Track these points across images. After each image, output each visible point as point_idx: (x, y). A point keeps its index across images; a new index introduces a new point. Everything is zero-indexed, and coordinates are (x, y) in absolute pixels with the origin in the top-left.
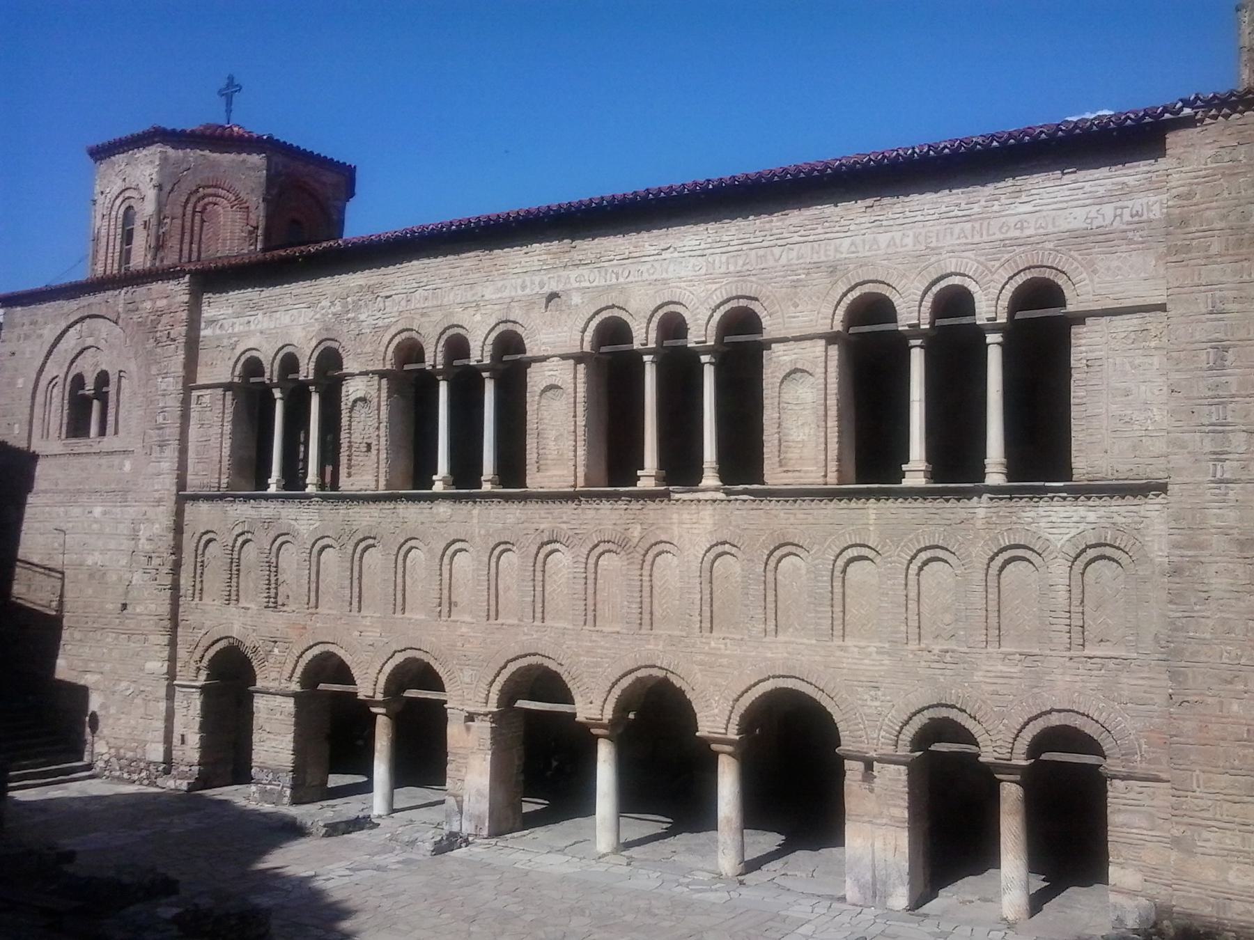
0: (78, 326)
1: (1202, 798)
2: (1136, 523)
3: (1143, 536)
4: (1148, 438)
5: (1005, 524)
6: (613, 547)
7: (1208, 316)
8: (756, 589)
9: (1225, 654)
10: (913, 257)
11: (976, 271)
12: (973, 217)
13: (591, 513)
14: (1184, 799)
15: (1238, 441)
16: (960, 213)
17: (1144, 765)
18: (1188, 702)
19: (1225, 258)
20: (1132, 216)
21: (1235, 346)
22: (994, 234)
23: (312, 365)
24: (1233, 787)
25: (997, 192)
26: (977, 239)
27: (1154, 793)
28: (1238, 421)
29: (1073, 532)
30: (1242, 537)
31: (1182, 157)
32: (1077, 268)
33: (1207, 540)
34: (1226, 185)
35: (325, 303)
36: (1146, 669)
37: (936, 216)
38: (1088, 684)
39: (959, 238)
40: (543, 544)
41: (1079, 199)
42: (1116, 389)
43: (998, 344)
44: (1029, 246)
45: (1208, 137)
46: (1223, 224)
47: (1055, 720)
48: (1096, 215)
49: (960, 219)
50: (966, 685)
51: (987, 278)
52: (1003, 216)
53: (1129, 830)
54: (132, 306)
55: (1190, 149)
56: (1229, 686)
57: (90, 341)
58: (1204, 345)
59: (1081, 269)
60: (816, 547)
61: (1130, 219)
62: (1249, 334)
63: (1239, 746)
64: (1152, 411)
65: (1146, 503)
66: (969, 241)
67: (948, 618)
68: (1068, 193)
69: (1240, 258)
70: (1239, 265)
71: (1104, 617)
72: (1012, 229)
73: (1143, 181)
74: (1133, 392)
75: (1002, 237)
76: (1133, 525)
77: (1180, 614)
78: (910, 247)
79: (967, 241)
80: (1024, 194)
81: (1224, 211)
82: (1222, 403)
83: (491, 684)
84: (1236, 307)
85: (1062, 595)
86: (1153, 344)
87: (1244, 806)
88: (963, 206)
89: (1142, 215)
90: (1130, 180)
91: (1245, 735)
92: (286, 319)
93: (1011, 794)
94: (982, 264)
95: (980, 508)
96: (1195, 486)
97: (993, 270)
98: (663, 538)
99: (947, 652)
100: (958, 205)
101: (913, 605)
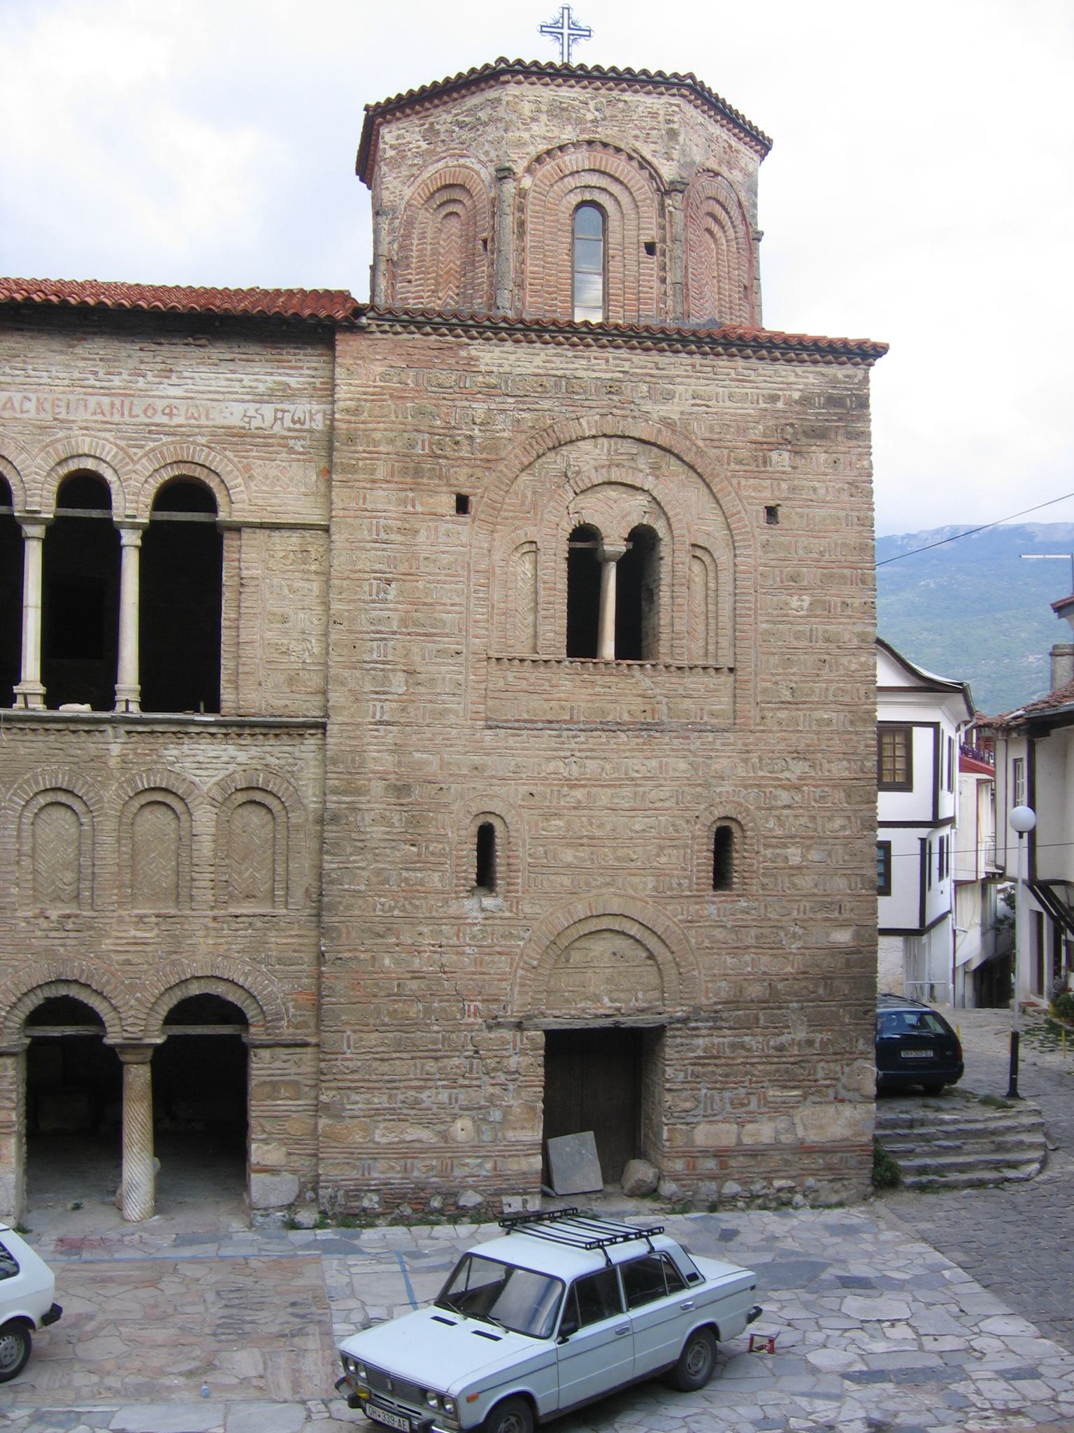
1: (351, 1060)
2: (290, 765)
3: (297, 779)
4: (304, 672)
5: (145, 763)
7: (372, 544)
9: (379, 906)
10: (34, 426)
11: (115, 456)
12: (113, 391)
14: (333, 1063)
15: (398, 684)
16: (98, 384)
17: (291, 1030)
18: (340, 959)
19: (390, 485)
20: (294, 422)
21: (397, 580)
22: (138, 416)
24: (383, 1044)
25: (142, 367)
26: (117, 418)
27: (301, 1059)
28: (397, 659)
29: (222, 774)
30: (399, 783)
31: (351, 368)
32: (232, 471)
33: (365, 785)
34: (393, 407)
36: (296, 926)
37: (66, 382)
38: (233, 946)
39: (95, 413)
41: (237, 393)
42: (274, 614)
43: (136, 546)
44: (178, 438)
45: (378, 353)
46: (390, 449)
47: (195, 989)
48: (254, 414)
49: (96, 390)
50: (92, 955)
51: (129, 468)
52: (150, 397)
53: (274, 1103)
55: (359, 362)
56: (379, 941)
58: (367, 576)
59: (236, 473)
61: (292, 426)
62: (411, 568)
63: (389, 1001)
64: (311, 642)
65: (302, 744)
66: (108, 419)
67: (69, 876)
68: (225, 383)
69: (405, 486)
70: (403, 495)
71: (251, 870)
72: (159, 413)
73: (307, 386)
74: (291, 619)
75: (147, 420)
76: (287, 767)
77: (335, 866)
78: (32, 414)
79: (105, 419)
80: (174, 375)
81: (391, 435)
82: (385, 639)
84: (399, 538)
85: (205, 847)
86: (313, 568)
87: (391, 1062)
88: (101, 375)
89: (303, 424)
90: (294, 382)
91: (396, 990)
93: (138, 1078)
94: (122, 449)
95: (115, 746)
96: (354, 727)
97: (135, 459)
99: (69, 917)
100: (96, 373)
101: (26, 862)
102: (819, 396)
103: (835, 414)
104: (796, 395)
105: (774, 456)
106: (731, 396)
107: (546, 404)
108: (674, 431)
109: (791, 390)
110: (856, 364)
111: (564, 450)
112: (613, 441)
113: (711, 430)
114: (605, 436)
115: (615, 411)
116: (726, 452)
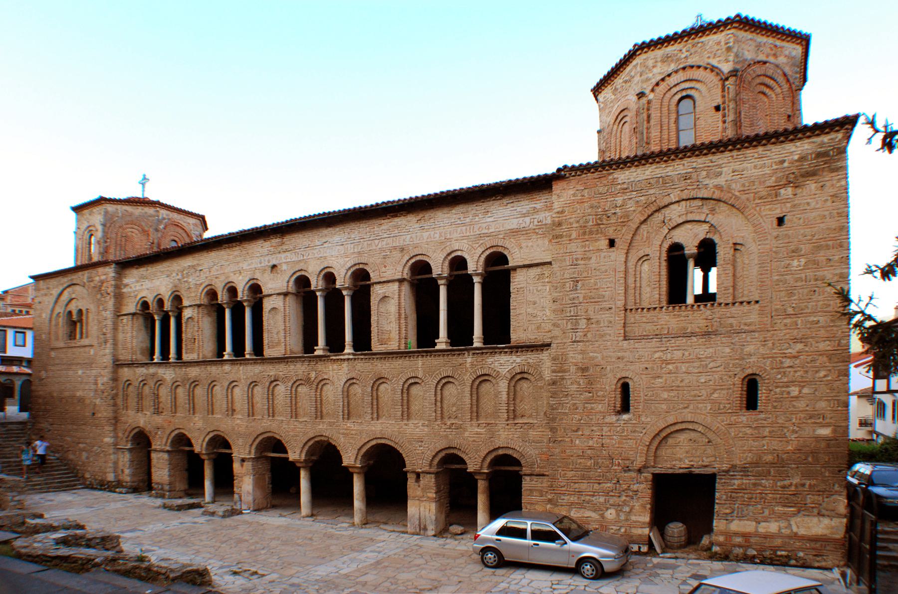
0: (68, 290)
6: (303, 382)
8: (368, 399)
13: (292, 367)
23: (169, 303)
35: (174, 274)
40: (272, 382)
54: (91, 280)
57: (73, 296)
60: (395, 379)
83: (251, 445)
92: (157, 283)
95: (469, 359)
98: (326, 377)
102: (811, 154)
103: (822, 161)
104: (796, 157)
105: (782, 191)
106: (755, 167)
107: (652, 191)
108: (722, 191)
109: (792, 155)
110: (837, 131)
111: (663, 211)
112: (688, 202)
113: (744, 185)
114: (683, 200)
115: (688, 187)
116: (752, 195)
